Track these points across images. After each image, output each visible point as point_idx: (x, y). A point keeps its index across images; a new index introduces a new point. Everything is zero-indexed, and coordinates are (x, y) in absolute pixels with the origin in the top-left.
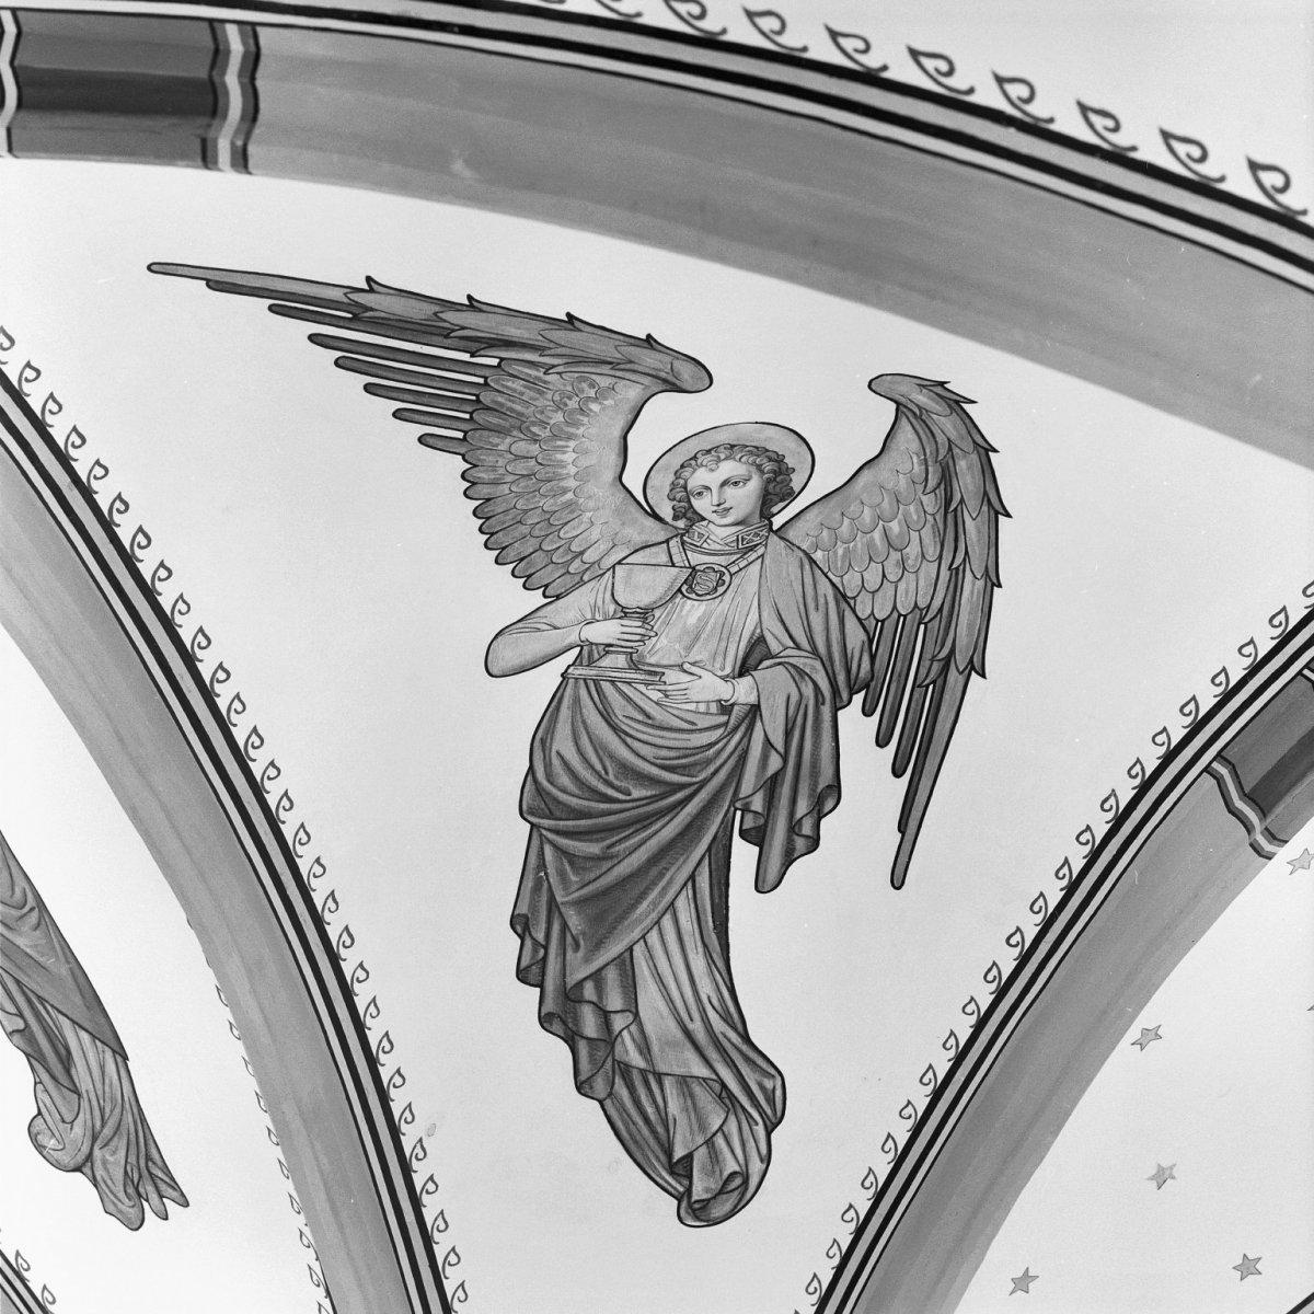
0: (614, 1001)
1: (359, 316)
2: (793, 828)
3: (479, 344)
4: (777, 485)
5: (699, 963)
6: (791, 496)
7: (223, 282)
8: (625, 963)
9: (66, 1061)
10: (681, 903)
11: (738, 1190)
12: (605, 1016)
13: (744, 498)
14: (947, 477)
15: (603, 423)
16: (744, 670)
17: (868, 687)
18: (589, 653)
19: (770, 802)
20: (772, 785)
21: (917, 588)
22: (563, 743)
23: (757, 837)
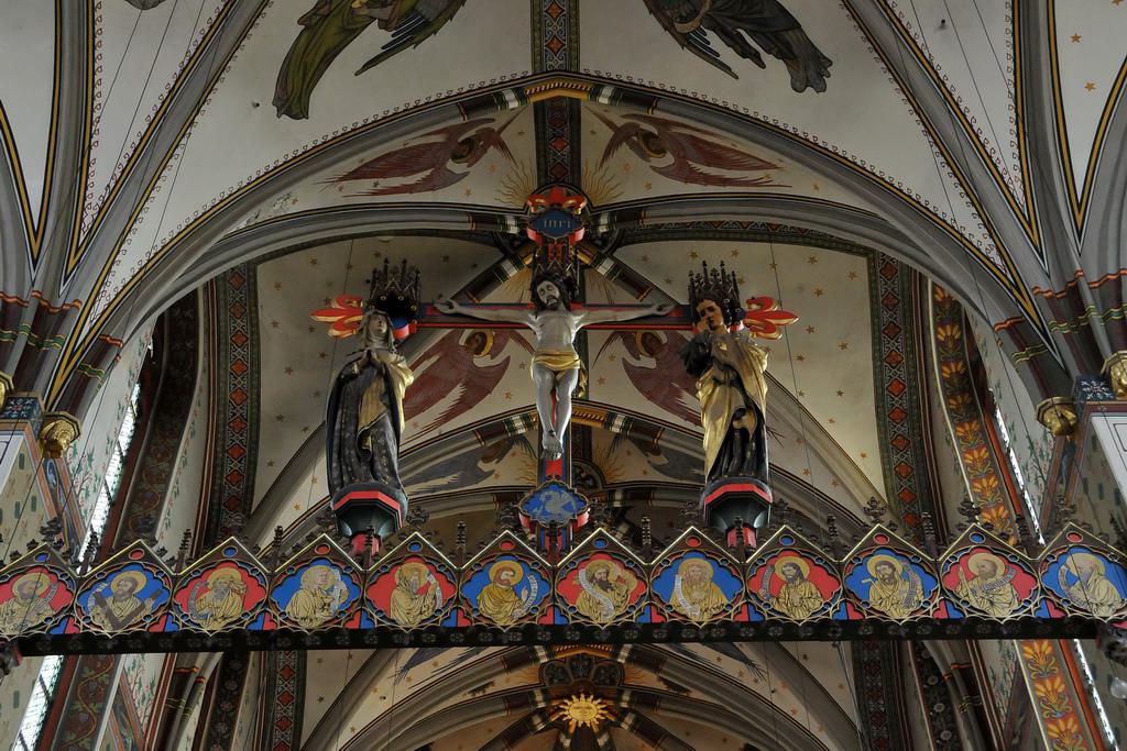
9: (788, 45)
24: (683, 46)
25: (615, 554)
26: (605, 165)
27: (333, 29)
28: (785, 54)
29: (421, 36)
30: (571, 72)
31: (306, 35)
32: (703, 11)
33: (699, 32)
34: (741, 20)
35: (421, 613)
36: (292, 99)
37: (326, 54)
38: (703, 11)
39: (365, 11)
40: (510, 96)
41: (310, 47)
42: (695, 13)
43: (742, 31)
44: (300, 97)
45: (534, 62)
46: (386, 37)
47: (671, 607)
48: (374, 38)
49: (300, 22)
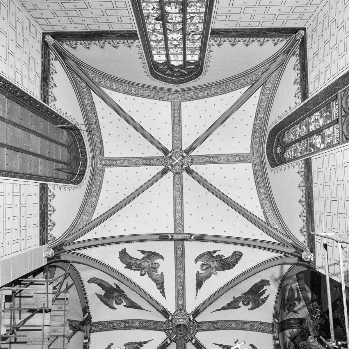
0: (233, 263)
1: (198, 288)
3: (198, 283)
4: (204, 264)
5: (229, 259)
7: (196, 295)
10: (227, 260)
11: (240, 252)
12: (234, 263)
13: (205, 266)
14: (200, 258)
15: (202, 275)
16: (214, 262)
17: (212, 255)
18: (215, 270)
20: (219, 258)
21: (206, 256)
22: (220, 270)
23: (222, 258)
26: (300, 313)
30: (272, 325)
34: (257, 293)
42: (258, 300)
43: (259, 293)
45: (270, 333)
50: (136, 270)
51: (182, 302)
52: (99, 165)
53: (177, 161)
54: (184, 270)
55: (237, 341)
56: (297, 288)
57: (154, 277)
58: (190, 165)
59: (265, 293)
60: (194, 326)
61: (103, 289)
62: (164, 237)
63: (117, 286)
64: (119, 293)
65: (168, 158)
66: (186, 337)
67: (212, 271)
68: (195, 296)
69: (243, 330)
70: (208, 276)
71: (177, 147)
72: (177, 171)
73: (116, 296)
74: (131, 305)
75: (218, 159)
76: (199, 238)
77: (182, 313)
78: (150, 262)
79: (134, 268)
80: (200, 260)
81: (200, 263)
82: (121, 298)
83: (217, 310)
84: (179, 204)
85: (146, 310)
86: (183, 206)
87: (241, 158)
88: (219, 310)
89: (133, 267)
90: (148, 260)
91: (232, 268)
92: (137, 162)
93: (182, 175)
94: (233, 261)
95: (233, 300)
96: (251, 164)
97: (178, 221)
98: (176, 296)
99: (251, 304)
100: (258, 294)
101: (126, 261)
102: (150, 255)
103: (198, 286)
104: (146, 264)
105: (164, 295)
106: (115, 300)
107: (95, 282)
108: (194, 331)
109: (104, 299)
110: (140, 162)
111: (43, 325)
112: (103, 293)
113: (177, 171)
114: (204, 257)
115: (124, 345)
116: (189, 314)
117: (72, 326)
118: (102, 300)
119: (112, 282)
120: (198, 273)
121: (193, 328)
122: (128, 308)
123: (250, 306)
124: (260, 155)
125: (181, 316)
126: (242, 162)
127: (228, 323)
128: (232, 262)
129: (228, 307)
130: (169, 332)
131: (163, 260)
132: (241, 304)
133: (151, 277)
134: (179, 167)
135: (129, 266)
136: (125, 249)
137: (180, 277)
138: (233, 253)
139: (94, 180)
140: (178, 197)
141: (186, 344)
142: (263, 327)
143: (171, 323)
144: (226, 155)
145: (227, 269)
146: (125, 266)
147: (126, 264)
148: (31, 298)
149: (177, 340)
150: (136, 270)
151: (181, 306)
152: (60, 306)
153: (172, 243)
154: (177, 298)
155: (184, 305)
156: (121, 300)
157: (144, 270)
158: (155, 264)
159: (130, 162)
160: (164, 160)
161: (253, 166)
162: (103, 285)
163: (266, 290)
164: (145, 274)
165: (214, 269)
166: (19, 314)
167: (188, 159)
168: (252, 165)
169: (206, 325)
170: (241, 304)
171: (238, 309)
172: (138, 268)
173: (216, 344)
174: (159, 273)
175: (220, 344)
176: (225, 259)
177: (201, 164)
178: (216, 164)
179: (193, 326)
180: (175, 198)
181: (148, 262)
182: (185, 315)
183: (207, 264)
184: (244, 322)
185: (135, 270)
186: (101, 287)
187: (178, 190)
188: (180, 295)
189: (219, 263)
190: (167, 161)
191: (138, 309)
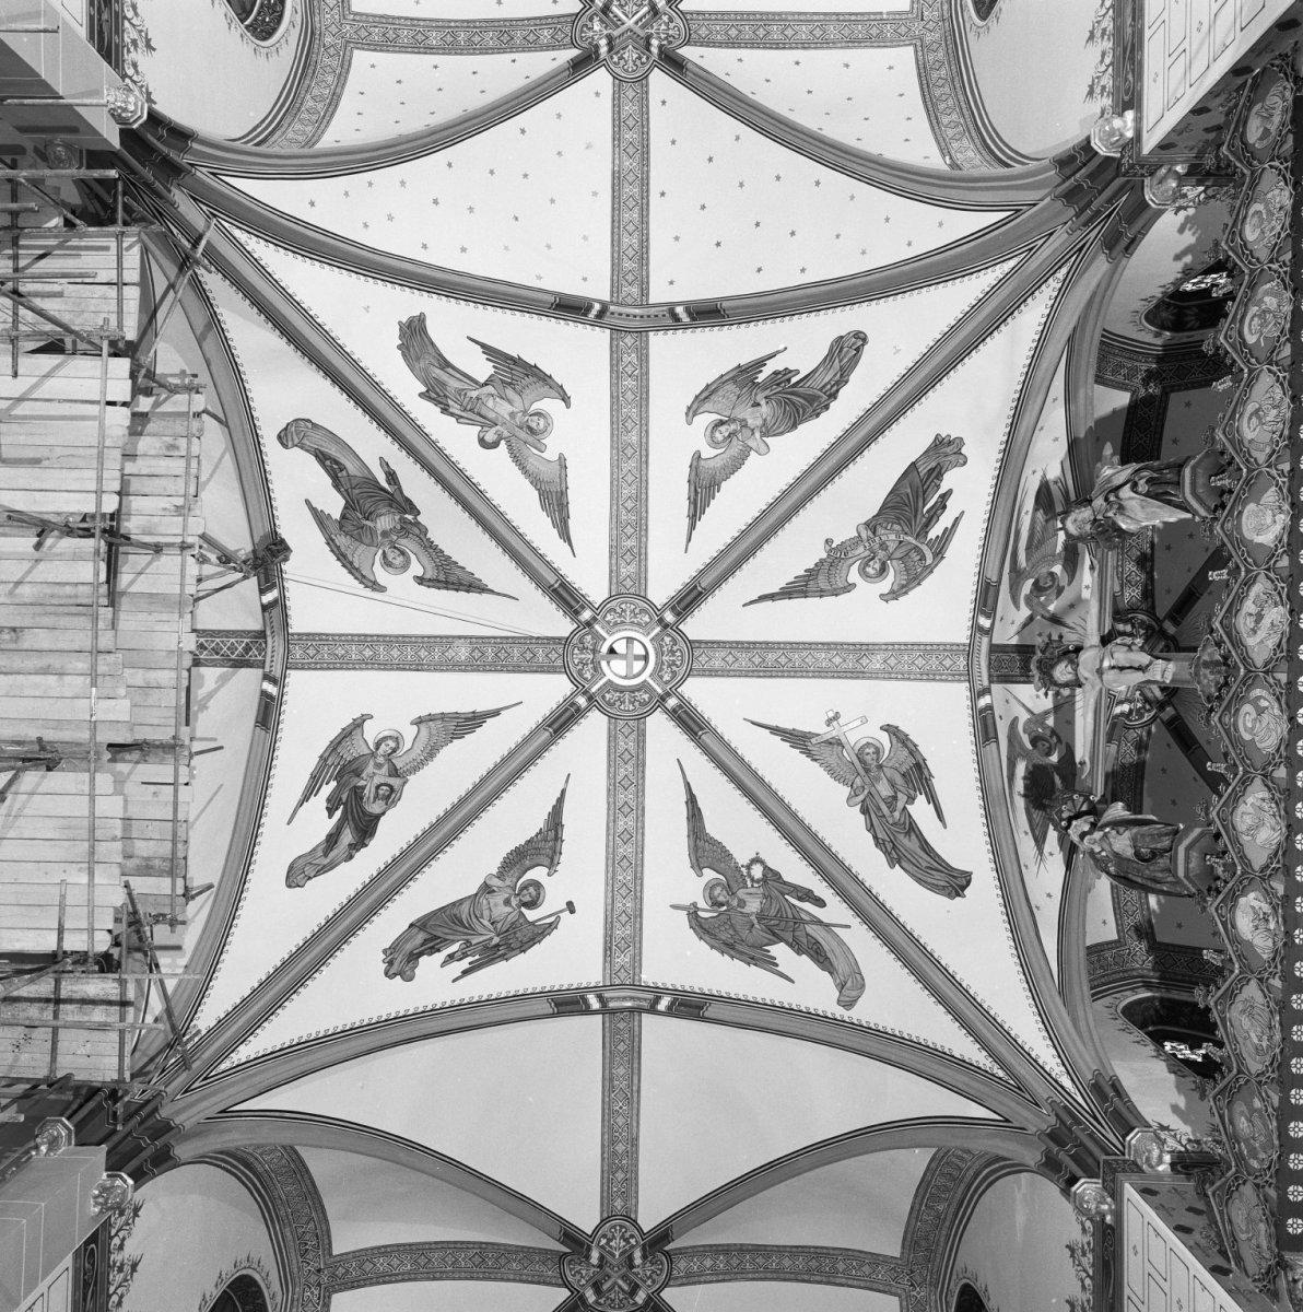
0: (829, 386)
1: (695, 515)
2: (785, 375)
4: (722, 423)
6: (721, 420)
7: (689, 540)
8: (821, 390)
9: (933, 470)
13: (723, 428)
14: (706, 398)
15: (711, 464)
16: (759, 405)
19: (781, 383)
20: (778, 385)
21: (731, 387)
22: (781, 429)
23: (789, 380)
24: (943, 558)
25: (1232, 610)
26: (1072, 625)
27: (905, 841)
28: (937, 473)
29: (925, 772)
30: (969, 651)
31: (904, 864)
32: (914, 542)
33: (930, 544)
34: (916, 511)
35: (1274, 816)
36: (955, 883)
37: (924, 850)
38: (914, 542)
39: (897, 814)
40: (984, 701)
41: (914, 861)
43: (925, 510)
44: (954, 877)
45: (959, 681)
46: (921, 799)
47: (1276, 545)
48: (920, 810)
49: (892, 866)
50: (462, 417)
51: (632, 569)
52: (328, 40)
53: (630, 23)
54: (644, 453)
55: (836, 717)
56: (1067, 492)
57: (532, 463)
58: (680, 46)
59: (944, 507)
60: (678, 654)
61: (337, 484)
62: (569, 308)
63: (392, 477)
64: (397, 518)
65: (596, 19)
66: (646, 692)
67: (751, 443)
68: (685, 543)
69: (858, 678)
70: (736, 464)
71: (631, 88)
72: (627, 71)
73: (385, 534)
74: (442, 578)
75: (786, 33)
76: (707, 314)
77: (633, 607)
78: (518, 404)
79: (455, 409)
80: (707, 406)
81: (705, 419)
82: (407, 544)
83: (762, 598)
84: (631, 203)
85: (499, 594)
86: (648, 210)
87: (874, 31)
88: (771, 597)
89: (450, 402)
90: (510, 392)
91: (827, 407)
92: (476, 39)
93: (647, 86)
94: (829, 382)
95: (825, 556)
96: (911, 48)
97: (627, 265)
98: (611, 547)
99: (892, 570)
100: (919, 516)
101: (426, 370)
102: (516, 372)
103: (696, 512)
104: (504, 409)
105: (565, 534)
106: (380, 552)
107: (305, 441)
108: (674, 674)
109: (342, 540)
110: (490, 38)
111: (103, 403)
112: (334, 505)
113: (627, 71)
114: (720, 393)
115: (412, 724)
116: (659, 607)
117: (217, 654)
118: (330, 542)
119: (371, 447)
120: (697, 456)
121: (674, 661)
122: (429, 587)
123: (886, 585)
124: (946, 15)
125: (628, 613)
126: (875, 44)
127: (805, 653)
128: (824, 386)
129: (800, 588)
130: (581, 675)
131: (568, 406)
132: (854, 576)
133: (517, 458)
134: (635, 56)
135: (435, 394)
136: (421, 319)
137: (630, 478)
138: (832, 346)
139: (311, 81)
140: (631, 178)
141: (644, 723)
142: (934, 662)
143: (589, 638)
144: (815, 18)
145: (806, 420)
146: (424, 389)
147: (426, 385)
148: (59, 299)
149: (611, 704)
150: (462, 420)
151: (628, 583)
152: (169, 440)
153: (603, 336)
154: (616, 551)
155: (641, 577)
156: (403, 553)
157: (494, 430)
158: (536, 418)
159: (449, 39)
160: (582, 31)
161: (920, 54)
162: (337, 463)
163: (950, 492)
164: (495, 445)
165: (757, 435)
166: (10, 359)
167: (671, 25)
168: (916, 51)
169: (723, 654)
170: (854, 576)
171: (843, 597)
172: (469, 415)
173: (753, 723)
174: (551, 454)
175: (773, 723)
176: (798, 382)
177: (720, 45)
178: (777, 48)
179: (673, 653)
180: (617, 179)
181: (510, 402)
182: (643, 611)
183: (732, 420)
184: (864, 649)
185: (459, 418)
186: (332, 477)
187: (631, 150)
188: (629, 543)
189: (779, 403)
190: (591, 34)
191: (468, 591)
